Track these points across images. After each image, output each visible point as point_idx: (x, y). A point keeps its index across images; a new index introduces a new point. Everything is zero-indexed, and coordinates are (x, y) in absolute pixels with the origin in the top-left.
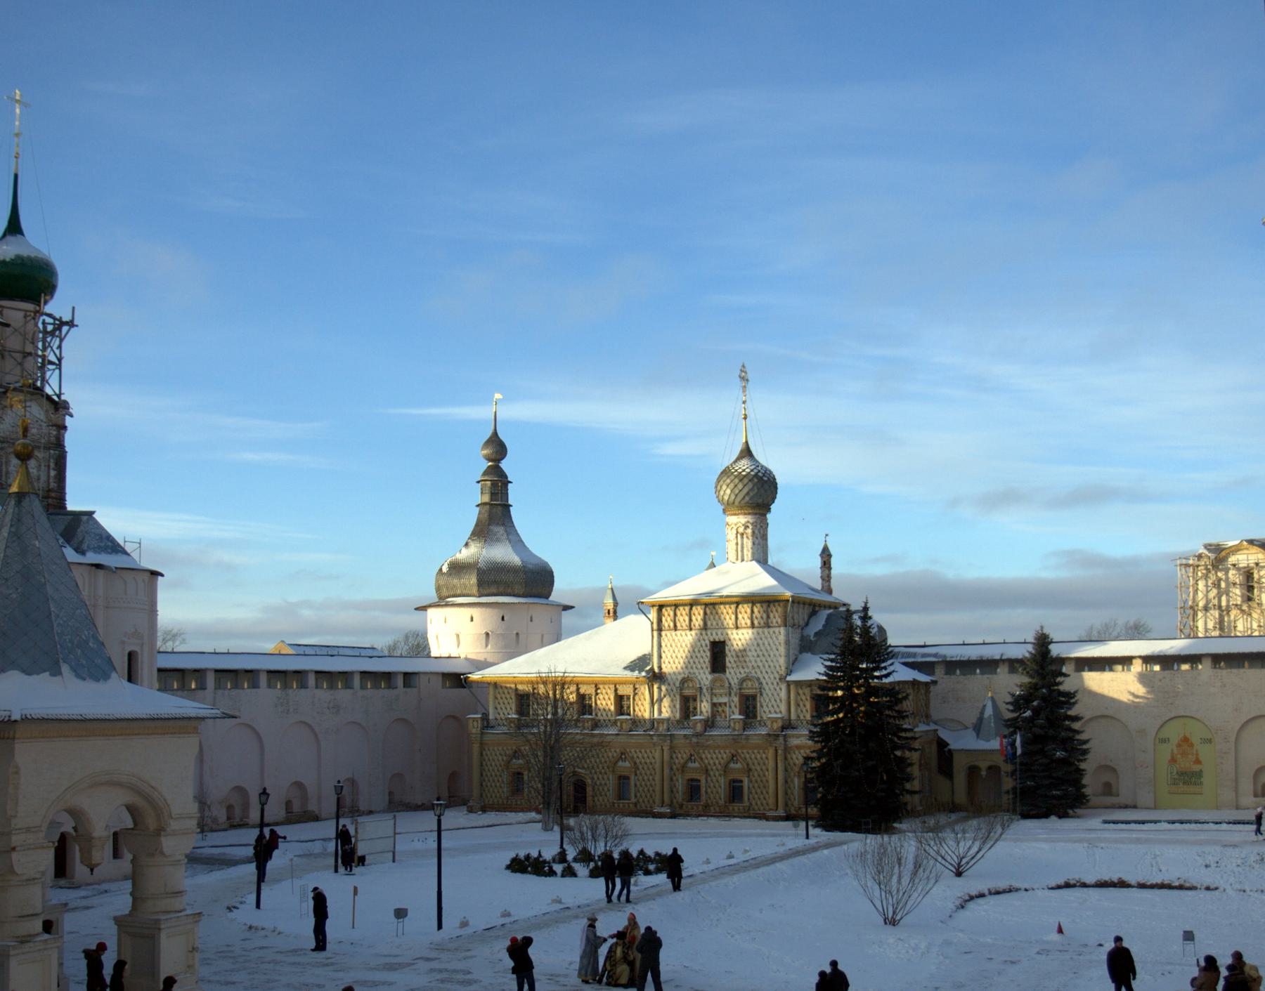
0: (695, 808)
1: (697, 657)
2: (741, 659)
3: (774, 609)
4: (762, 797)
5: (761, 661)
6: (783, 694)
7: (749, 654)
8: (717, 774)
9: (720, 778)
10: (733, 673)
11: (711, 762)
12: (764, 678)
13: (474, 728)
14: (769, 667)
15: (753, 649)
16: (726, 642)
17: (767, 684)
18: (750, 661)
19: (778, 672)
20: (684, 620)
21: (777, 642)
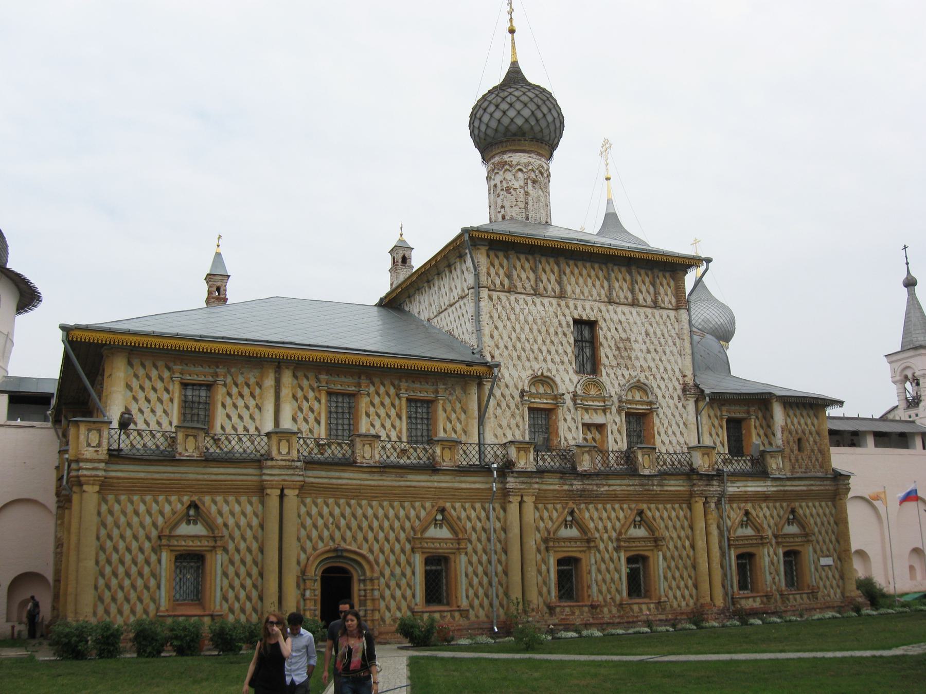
0: (577, 613)
1: (552, 342)
2: (624, 354)
3: (665, 282)
4: (682, 584)
5: (654, 360)
6: (692, 417)
7: (635, 346)
8: (610, 548)
9: (615, 555)
10: (612, 376)
11: (600, 526)
12: (659, 387)
13: (89, 445)
14: (665, 369)
15: (640, 339)
16: (600, 323)
17: (664, 397)
18: (637, 358)
19: (677, 379)
20: (528, 278)
21: (673, 333)
